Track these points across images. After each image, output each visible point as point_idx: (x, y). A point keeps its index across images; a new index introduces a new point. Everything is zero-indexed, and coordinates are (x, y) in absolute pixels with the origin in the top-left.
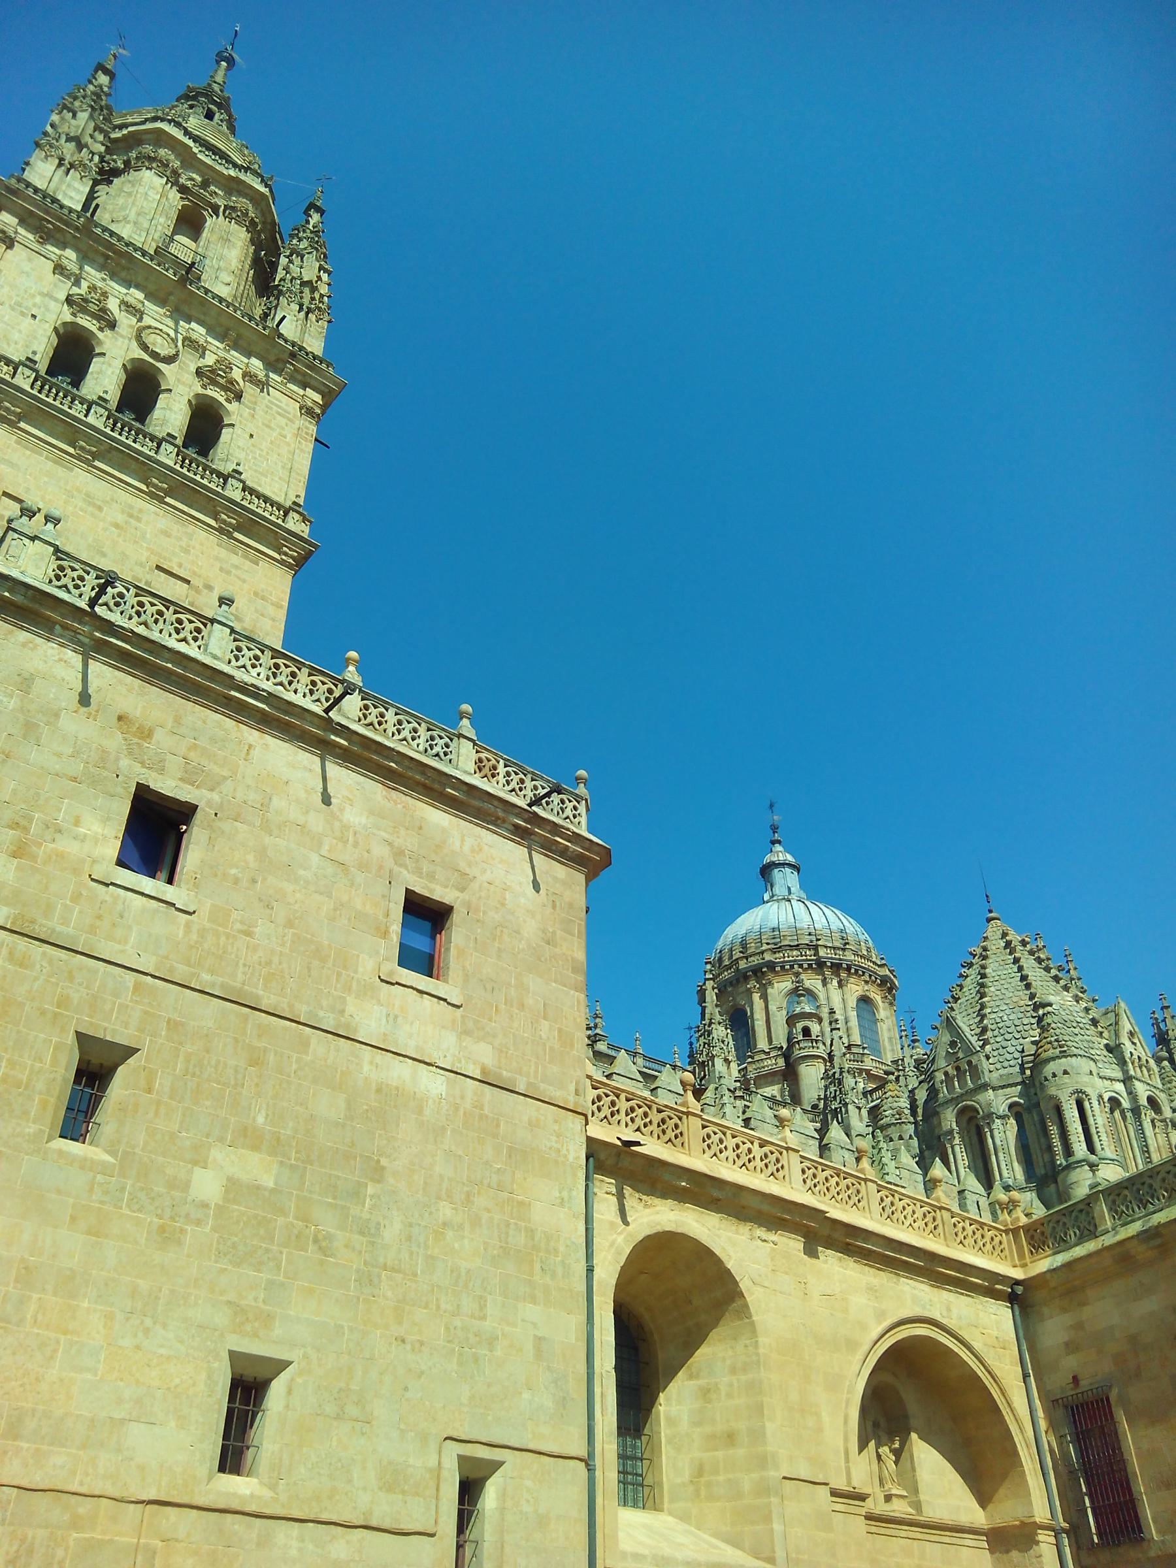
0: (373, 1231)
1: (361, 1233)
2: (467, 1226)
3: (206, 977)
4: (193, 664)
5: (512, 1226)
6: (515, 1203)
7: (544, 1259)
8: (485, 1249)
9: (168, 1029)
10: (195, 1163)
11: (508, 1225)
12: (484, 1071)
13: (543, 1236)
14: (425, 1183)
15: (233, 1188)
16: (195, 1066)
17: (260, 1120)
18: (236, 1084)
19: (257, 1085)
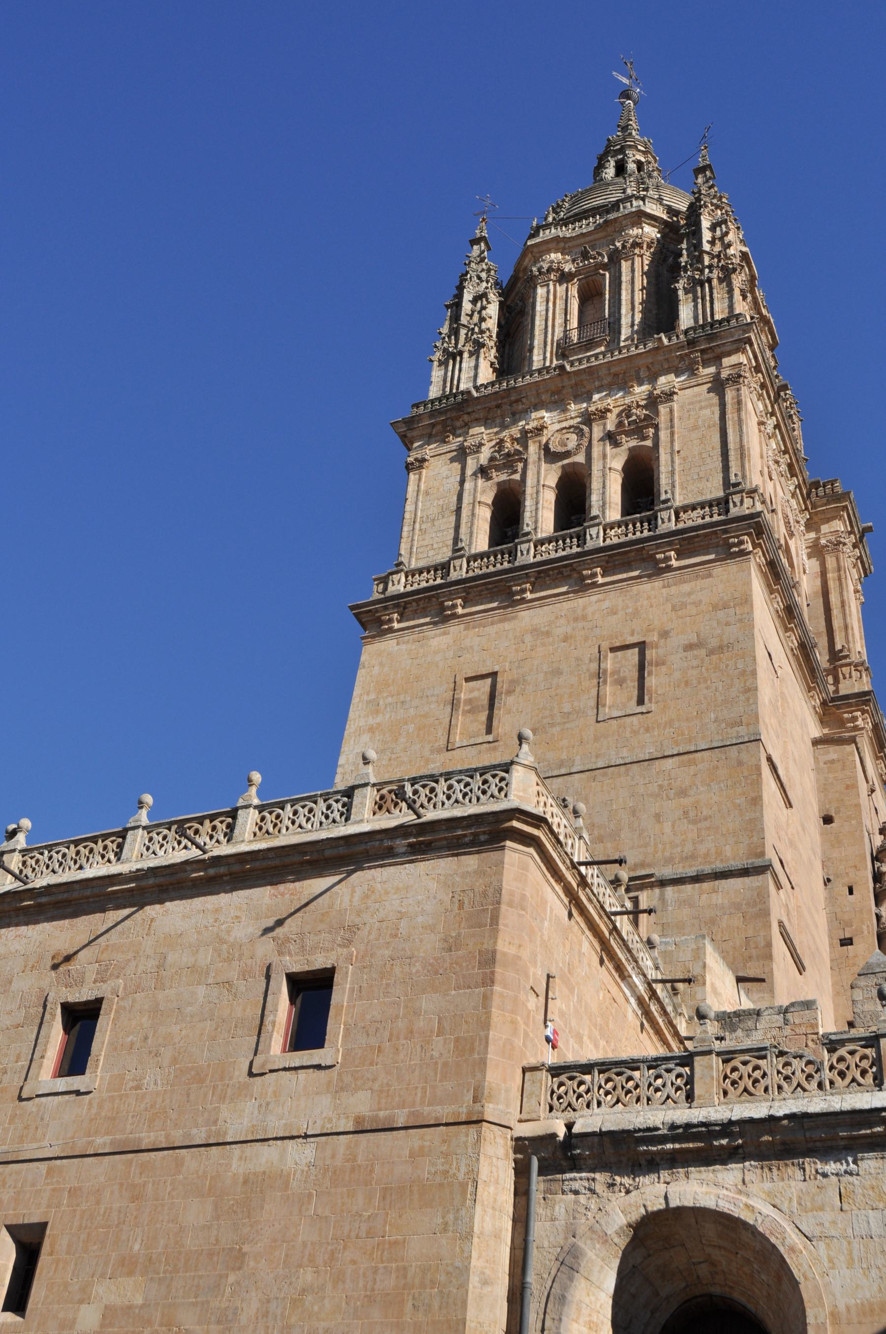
0: (230, 1317)
1: (219, 1322)
2: (329, 1286)
3: (99, 1140)
4: (95, 882)
5: (381, 1271)
6: (387, 1246)
7: (417, 1295)
8: (347, 1303)
9: (69, 1196)
10: (81, 1302)
11: (375, 1271)
12: (358, 1120)
13: (418, 1270)
14: (287, 1255)
15: (109, 1314)
16: (87, 1220)
17: (137, 1247)
18: (119, 1224)
19: (136, 1217)
